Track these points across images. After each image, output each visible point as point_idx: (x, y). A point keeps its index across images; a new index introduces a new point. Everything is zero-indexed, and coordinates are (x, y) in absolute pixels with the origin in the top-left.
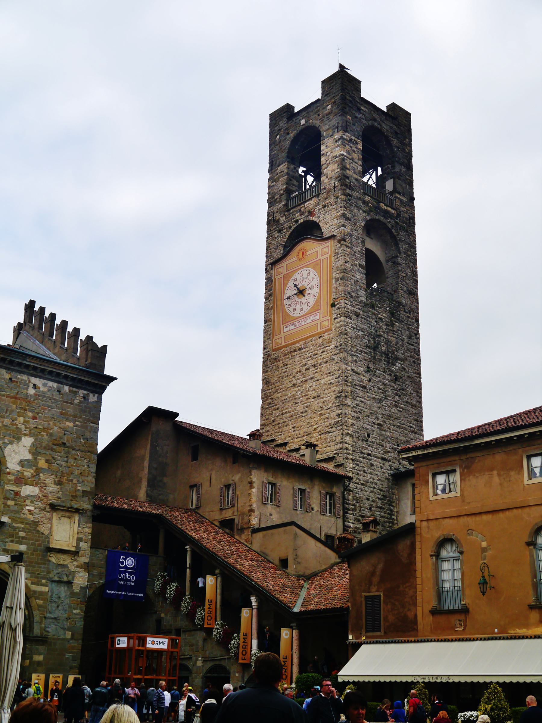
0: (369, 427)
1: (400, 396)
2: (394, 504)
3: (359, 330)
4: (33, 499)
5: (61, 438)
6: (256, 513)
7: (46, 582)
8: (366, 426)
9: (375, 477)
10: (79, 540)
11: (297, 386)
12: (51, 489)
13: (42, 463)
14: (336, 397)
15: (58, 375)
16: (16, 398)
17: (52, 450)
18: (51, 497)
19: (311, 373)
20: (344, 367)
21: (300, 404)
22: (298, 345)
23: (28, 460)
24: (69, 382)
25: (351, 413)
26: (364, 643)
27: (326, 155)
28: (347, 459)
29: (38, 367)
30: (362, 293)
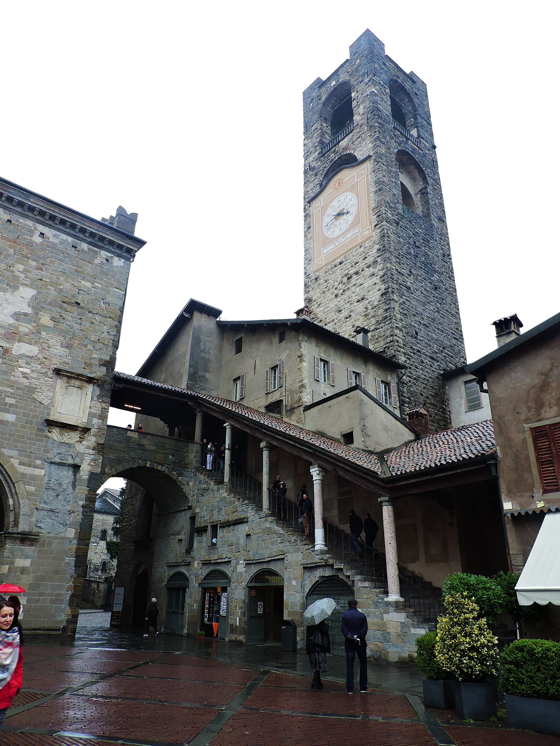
0: (416, 325)
1: (440, 304)
2: (446, 404)
3: (400, 237)
4: (30, 359)
5: (74, 296)
6: (308, 390)
7: (42, 464)
8: (413, 324)
9: (427, 374)
10: (91, 415)
11: (339, 296)
12: (56, 351)
13: (45, 320)
14: (382, 295)
15: (73, 226)
16: (15, 242)
17: (61, 308)
18: (55, 361)
19: (353, 281)
20: (388, 265)
21: (343, 311)
22: (339, 260)
23: (25, 314)
24: (87, 239)
25: (399, 308)
26: (550, 511)
27: (357, 98)
28: (398, 351)
29: (46, 212)
30: (400, 206)
